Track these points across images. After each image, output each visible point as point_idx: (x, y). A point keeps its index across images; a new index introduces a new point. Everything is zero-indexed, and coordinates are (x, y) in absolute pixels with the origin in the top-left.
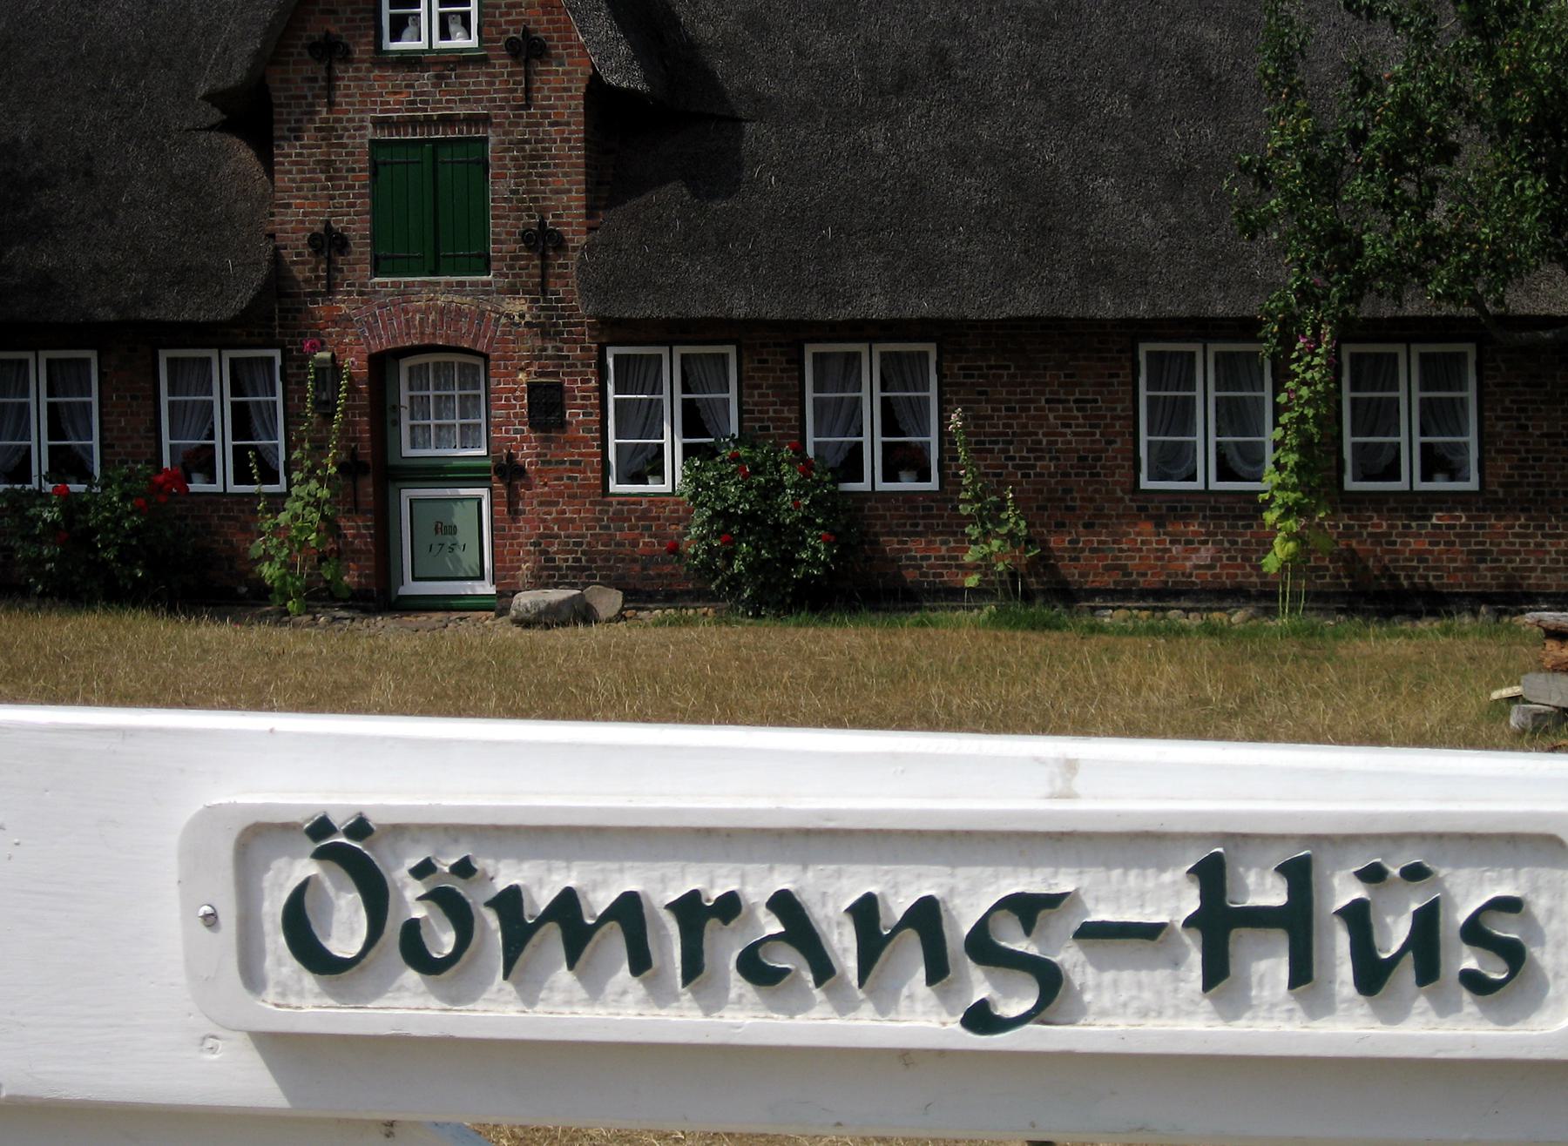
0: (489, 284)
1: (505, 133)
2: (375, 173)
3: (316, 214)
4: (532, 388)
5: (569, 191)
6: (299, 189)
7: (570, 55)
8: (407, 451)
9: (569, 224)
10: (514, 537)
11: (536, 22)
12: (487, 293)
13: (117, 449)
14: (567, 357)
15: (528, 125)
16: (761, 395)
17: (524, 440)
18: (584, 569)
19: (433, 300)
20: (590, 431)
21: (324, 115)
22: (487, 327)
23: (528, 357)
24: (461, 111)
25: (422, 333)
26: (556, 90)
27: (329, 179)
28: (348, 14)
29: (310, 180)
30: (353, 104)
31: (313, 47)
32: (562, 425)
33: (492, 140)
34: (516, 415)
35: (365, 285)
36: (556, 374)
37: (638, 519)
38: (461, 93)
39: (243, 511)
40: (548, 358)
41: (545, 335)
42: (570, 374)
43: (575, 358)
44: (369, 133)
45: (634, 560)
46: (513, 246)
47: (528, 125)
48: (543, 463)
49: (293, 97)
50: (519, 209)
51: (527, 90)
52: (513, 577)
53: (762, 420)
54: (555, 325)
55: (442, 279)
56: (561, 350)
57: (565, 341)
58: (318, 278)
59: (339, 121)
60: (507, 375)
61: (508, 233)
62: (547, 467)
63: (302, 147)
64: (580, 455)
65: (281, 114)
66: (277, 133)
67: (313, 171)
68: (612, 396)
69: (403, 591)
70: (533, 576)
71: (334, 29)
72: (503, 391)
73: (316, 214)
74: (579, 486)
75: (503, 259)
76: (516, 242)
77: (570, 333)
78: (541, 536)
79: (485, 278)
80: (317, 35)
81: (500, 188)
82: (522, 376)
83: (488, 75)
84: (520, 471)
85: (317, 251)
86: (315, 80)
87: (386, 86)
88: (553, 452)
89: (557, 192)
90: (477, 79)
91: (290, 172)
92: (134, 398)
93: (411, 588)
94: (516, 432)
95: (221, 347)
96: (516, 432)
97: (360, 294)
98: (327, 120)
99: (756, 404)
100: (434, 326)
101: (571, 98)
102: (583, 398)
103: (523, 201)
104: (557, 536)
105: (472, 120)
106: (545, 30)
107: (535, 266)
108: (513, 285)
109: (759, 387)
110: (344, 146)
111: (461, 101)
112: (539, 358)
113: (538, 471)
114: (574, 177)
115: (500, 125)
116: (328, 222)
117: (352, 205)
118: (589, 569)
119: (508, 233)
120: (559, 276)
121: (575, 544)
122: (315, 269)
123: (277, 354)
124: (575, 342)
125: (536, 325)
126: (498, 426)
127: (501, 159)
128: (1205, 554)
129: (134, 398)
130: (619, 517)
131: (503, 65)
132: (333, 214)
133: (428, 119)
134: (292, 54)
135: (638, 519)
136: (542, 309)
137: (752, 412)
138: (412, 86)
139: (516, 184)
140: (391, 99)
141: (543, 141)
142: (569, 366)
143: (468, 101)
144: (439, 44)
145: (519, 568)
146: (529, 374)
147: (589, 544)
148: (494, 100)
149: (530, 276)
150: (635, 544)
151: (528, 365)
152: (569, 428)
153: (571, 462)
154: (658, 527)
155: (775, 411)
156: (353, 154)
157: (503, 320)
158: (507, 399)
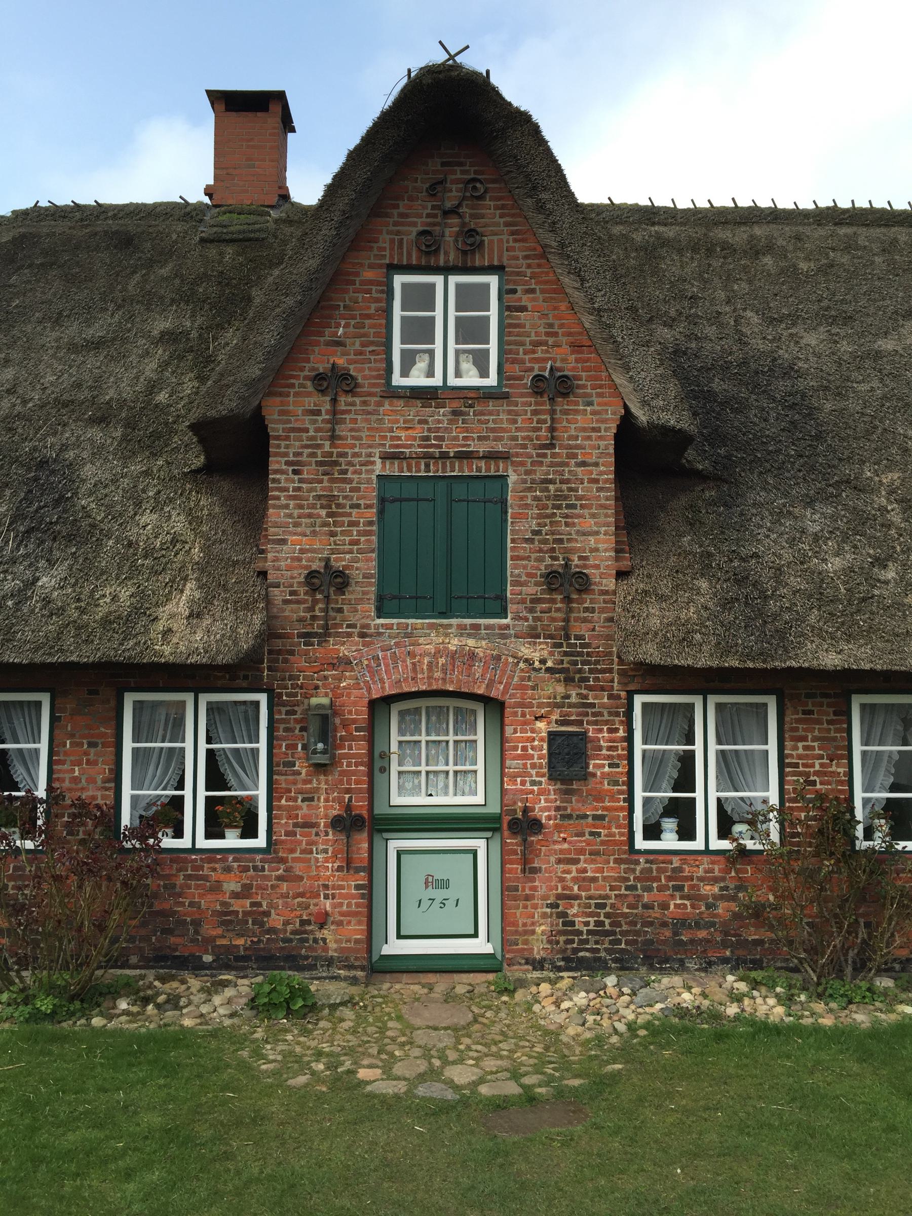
0: (507, 627)
1: (527, 473)
2: (381, 512)
5: (597, 533)
6: (296, 525)
7: (599, 395)
8: (396, 800)
9: (597, 567)
10: (527, 898)
11: (564, 360)
12: (504, 637)
14: (593, 705)
15: (552, 465)
16: (806, 748)
17: (541, 792)
18: (607, 933)
19: (439, 643)
20: (616, 783)
21: (327, 448)
22: (504, 672)
23: (548, 705)
24: (482, 448)
26: (584, 429)
27: (329, 515)
28: (357, 346)
29: (310, 516)
30: (360, 438)
31: (319, 379)
32: (586, 776)
33: (513, 478)
34: (533, 766)
35: (367, 626)
36: (580, 723)
37: (669, 879)
39: (214, 870)
40: (570, 706)
41: (568, 680)
42: (596, 723)
43: (603, 706)
44: (378, 468)
45: (664, 924)
47: (552, 465)
48: (563, 817)
50: (540, 550)
51: (552, 429)
52: (526, 942)
53: (808, 774)
54: (580, 671)
55: (454, 621)
56: (586, 697)
57: (590, 688)
58: (314, 618)
59: (344, 455)
60: (525, 723)
62: (566, 822)
63: (301, 481)
65: (279, 446)
66: (272, 467)
67: (313, 506)
68: (639, 747)
69: (387, 950)
70: (549, 942)
71: (341, 361)
72: (520, 740)
74: (603, 843)
75: (523, 601)
76: (536, 584)
77: (596, 679)
78: (559, 897)
79: (504, 621)
81: (520, 525)
82: (541, 725)
83: (509, 412)
84: (535, 825)
85: (314, 590)
86: (318, 413)
87: (397, 421)
88: (575, 805)
90: (499, 415)
91: (287, 506)
92: (92, 745)
93: (395, 947)
94: (533, 783)
96: (533, 783)
97: (362, 635)
98: (331, 454)
99: (800, 757)
100: (444, 671)
101: (600, 438)
102: (610, 748)
103: (545, 542)
104: (577, 897)
105: (491, 456)
106: (574, 369)
107: (558, 610)
108: (533, 628)
109: (804, 739)
110: (350, 481)
111: (480, 439)
113: (556, 826)
114: (602, 519)
115: (522, 464)
116: (328, 560)
117: (357, 542)
118: (613, 933)
119: (529, 575)
120: (585, 620)
121: (598, 906)
122: (312, 609)
123: (262, 698)
124: (602, 689)
125: (560, 671)
126: (514, 777)
127: (522, 498)
129: (92, 745)
130: (647, 877)
131: (525, 404)
132: (333, 552)
133: (444, 456)
134: (293, 386)
135: (669, 879)
136: (566, 654)
137: (796, 765)
138: (426, 422)
139: (539, 524)
140: (403, 434)
141: (568, 481)
142: (594, 714)
143: (486, 438)
144: (453, 381)
145: (533, 932)
146: (549, 723)
147: (613, 906)
148: (515, 438)
149: (553, 620)
150: (665, 906)
151: (550, 713)
152: (591, 780)
153: (595, 817)
154: (692, 887)
155: (821, 765)
156: (358, 490)
157: (522, 665)
158: (524, 749)
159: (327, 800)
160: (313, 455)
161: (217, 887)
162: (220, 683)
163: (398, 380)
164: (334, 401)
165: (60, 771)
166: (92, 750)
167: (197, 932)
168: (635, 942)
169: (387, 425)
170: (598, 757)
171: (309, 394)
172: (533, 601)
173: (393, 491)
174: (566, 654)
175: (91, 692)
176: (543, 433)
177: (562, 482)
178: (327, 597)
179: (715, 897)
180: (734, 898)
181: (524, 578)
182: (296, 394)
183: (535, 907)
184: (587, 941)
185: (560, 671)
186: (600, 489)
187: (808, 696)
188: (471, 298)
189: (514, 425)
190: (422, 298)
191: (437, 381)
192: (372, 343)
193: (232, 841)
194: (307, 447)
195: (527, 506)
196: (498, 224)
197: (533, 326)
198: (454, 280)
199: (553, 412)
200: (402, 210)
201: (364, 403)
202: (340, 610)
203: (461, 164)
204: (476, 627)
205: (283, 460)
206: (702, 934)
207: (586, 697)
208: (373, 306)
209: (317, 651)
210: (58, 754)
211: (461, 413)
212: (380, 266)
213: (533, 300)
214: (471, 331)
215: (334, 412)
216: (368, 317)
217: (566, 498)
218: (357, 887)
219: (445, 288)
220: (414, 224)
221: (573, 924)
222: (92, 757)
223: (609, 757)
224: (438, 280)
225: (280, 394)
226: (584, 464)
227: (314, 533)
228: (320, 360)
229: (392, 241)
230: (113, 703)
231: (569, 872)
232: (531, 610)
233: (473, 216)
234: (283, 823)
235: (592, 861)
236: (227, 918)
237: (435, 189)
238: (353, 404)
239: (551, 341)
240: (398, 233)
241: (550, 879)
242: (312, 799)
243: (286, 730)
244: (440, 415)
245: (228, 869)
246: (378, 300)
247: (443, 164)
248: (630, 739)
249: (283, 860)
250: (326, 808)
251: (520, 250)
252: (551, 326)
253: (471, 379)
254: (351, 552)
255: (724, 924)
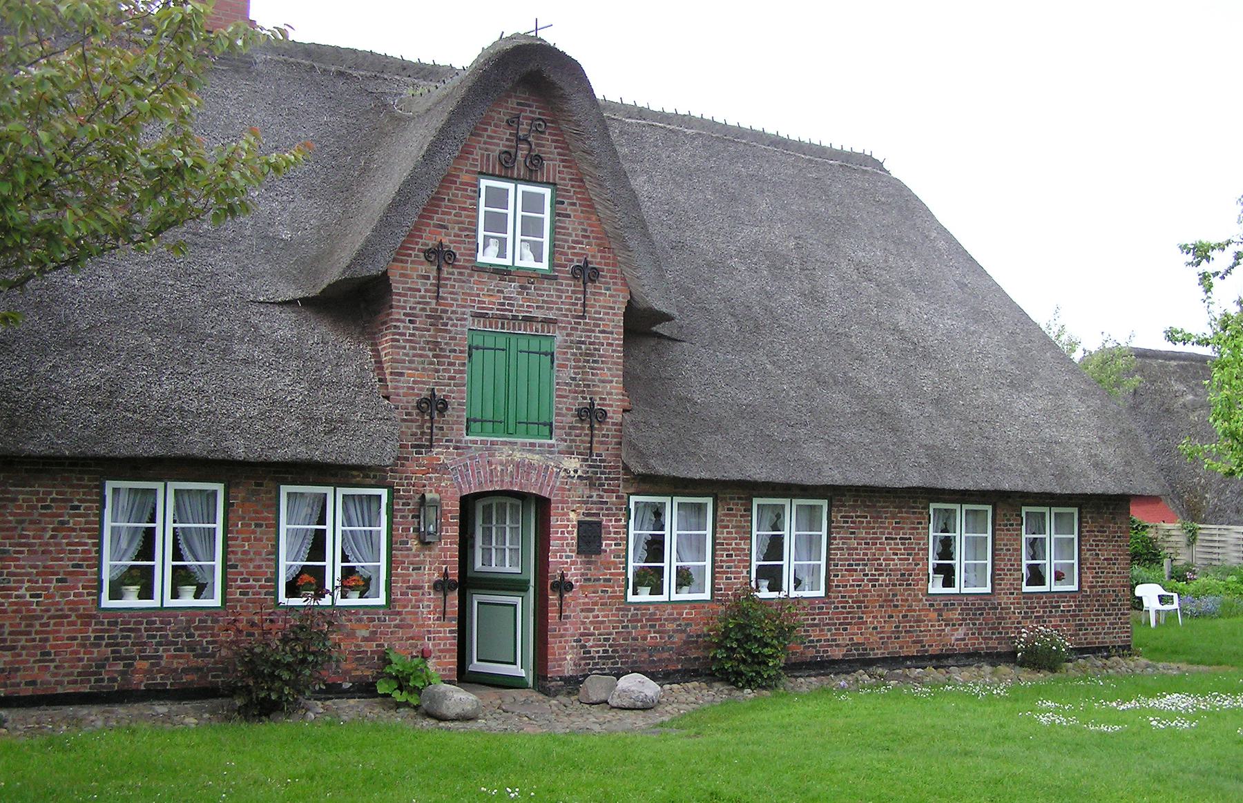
1: (568, 335)
3: (424, 383)
4: (580, 524)
7: (615, 284)
9: (611, 406)
11: (593, 256)
12: (551, 453)
13: (240, 569)
17: (573, 563)
21: (433, 306)
22: (550, 477)
23: (579, 502)
25: (502, 481)
26: (605, 307)
29: (421, 356)
30: (456, 300)
31: (428, 253)
32: (599, 551)
35: (460, 441)
38: (538, 301)
41: (592, 485)
42: (608, 515)
43: (613, 504)
45: (644, 650)
46: (570, 419)
49: (410, 289)
50: (576, 392)
51: (584, 305)
52: (560, 666)
54: (600, 478)
55: (519, 440)
56: (602, 497)
61: (568, 409)
63: (414, 329)
64: (611, 574)
67: (423, 349)
70: (575, 665)
71: (446, 241)
73: (424, 383)
78: (582, 635)
80: (431, 244)
83: (558, 290)
85: (422, 411)
86: (428, 278)
89: (603, 382)
90: (549, 290)
91: (404, 348)
94: (567, 557)
95: (337, 485)
96: (567, 557)
97: (456, 448)
102: (616, 533)
103: (579, 386)
104: (592, 634)
105: (546, 321)
106: (600, 263)
110: (450, 332)
112: (586, 503)
114: (615, 372)
117: (453, 378)
119: (568, 409)
120: (602, 443)
121: (605, 640)
122: (421, 427)
123: (384, 492)
124: (613, 491)
125: (586, 479)
128: (960, 633)
130: (635, 620)
131: (568, 285)
132: (437, 384)
133: (515, 318)
136: (590, 466)
140: (486, 300)
143: (542, 308)
144: (518, 263)
148: (561, 309)
149: (583, 442)
150: (645, 639)
153: (605, 580)
154: (660, 625)
157: (562, 474)
158: (562, 533)
159: (430, 569)
160: (423, 310)
161: (351, 635)
162: (354, 481)
163: (481, 258)
164: (439, 269)
165: (233, 546)
166: (258, 530)
167: (338, 667)
168: (626, 662)
169: (475, 292)
170: (608, 539)
171: (421, 263)
172: (570, 428)
173: (478, 341)
174: (590, 466)
175: (258, 485)
176: (578, 307)
177: (590, 343)
178: (432, 418)
179: (674, 631)
180: (684, 631)
181: (564, 411)
182: (413, 262)
183: (566, 642)
184: (597, 664)
185: (586, 479)
186: (614, 351)
187: (731, 499)
188: (532, 203)
189: (559, 300)
190: (498, 198)
191: (507, 262)
192: (466, 229)
193: (354, 600)
194: (419, 303)
195: (568, 360)
196: (551, 153)
197: (574, 229)
198: (522, 188)
199: (585, 293)
200: (489, 133)
201: (461, 274)
202: (441, 429)
203: (529, 106)
204: (533, 445)
205: (402, 312)
206: (666, 655)
207: (602, 497)
208: (469, 201)
209: (424, 458)
210: (231, 532)
211: (526, 288)
212: (474, 172)
213: (575, 211)
214: (531, 227)
215: (439, 278)
216: (465, 209)
217: (593, 355)
218: (451, 632)
219: (515, 192)
220: (498, 145)
221: (589, 652)
222: (258, 535)
223: (615, 539)
224: (510, 186)
225: (402, 261)
226: (603, 332)
227: (424, 369)
228: (429, 239)
229: (482, 155)
230: (273, 494)
231: (587, 618)
232: (569, 434)
233: (537, 145)
234: (398, 585)
235: (603, 610)
236: (359, 657)
237: (513, 122)
238: (453, 274)
239: (585, 241)
240: (487, 150)
241: (576, 623)
242: (419, 569)
243: (402, 517)
244: (512, 288)
245: (360, 620)
246: (472, 198)
247: (518, 104)
248: (627, 527)
249: (399, 613)
250: (430, 575)
251: (568, 173)
252: (586, 231)
253: (528, 262)
254: (449, 385)
255: (678, 648)
